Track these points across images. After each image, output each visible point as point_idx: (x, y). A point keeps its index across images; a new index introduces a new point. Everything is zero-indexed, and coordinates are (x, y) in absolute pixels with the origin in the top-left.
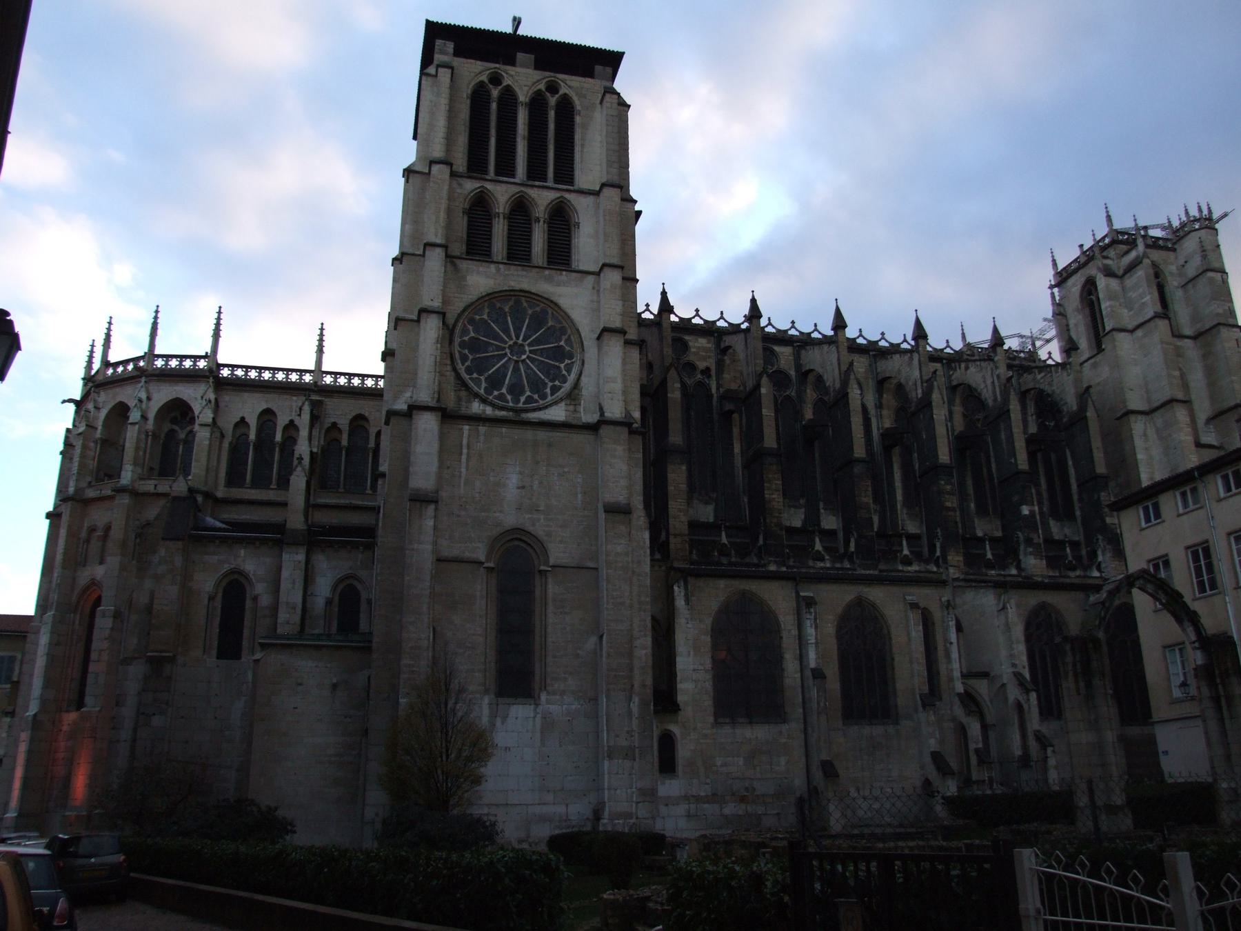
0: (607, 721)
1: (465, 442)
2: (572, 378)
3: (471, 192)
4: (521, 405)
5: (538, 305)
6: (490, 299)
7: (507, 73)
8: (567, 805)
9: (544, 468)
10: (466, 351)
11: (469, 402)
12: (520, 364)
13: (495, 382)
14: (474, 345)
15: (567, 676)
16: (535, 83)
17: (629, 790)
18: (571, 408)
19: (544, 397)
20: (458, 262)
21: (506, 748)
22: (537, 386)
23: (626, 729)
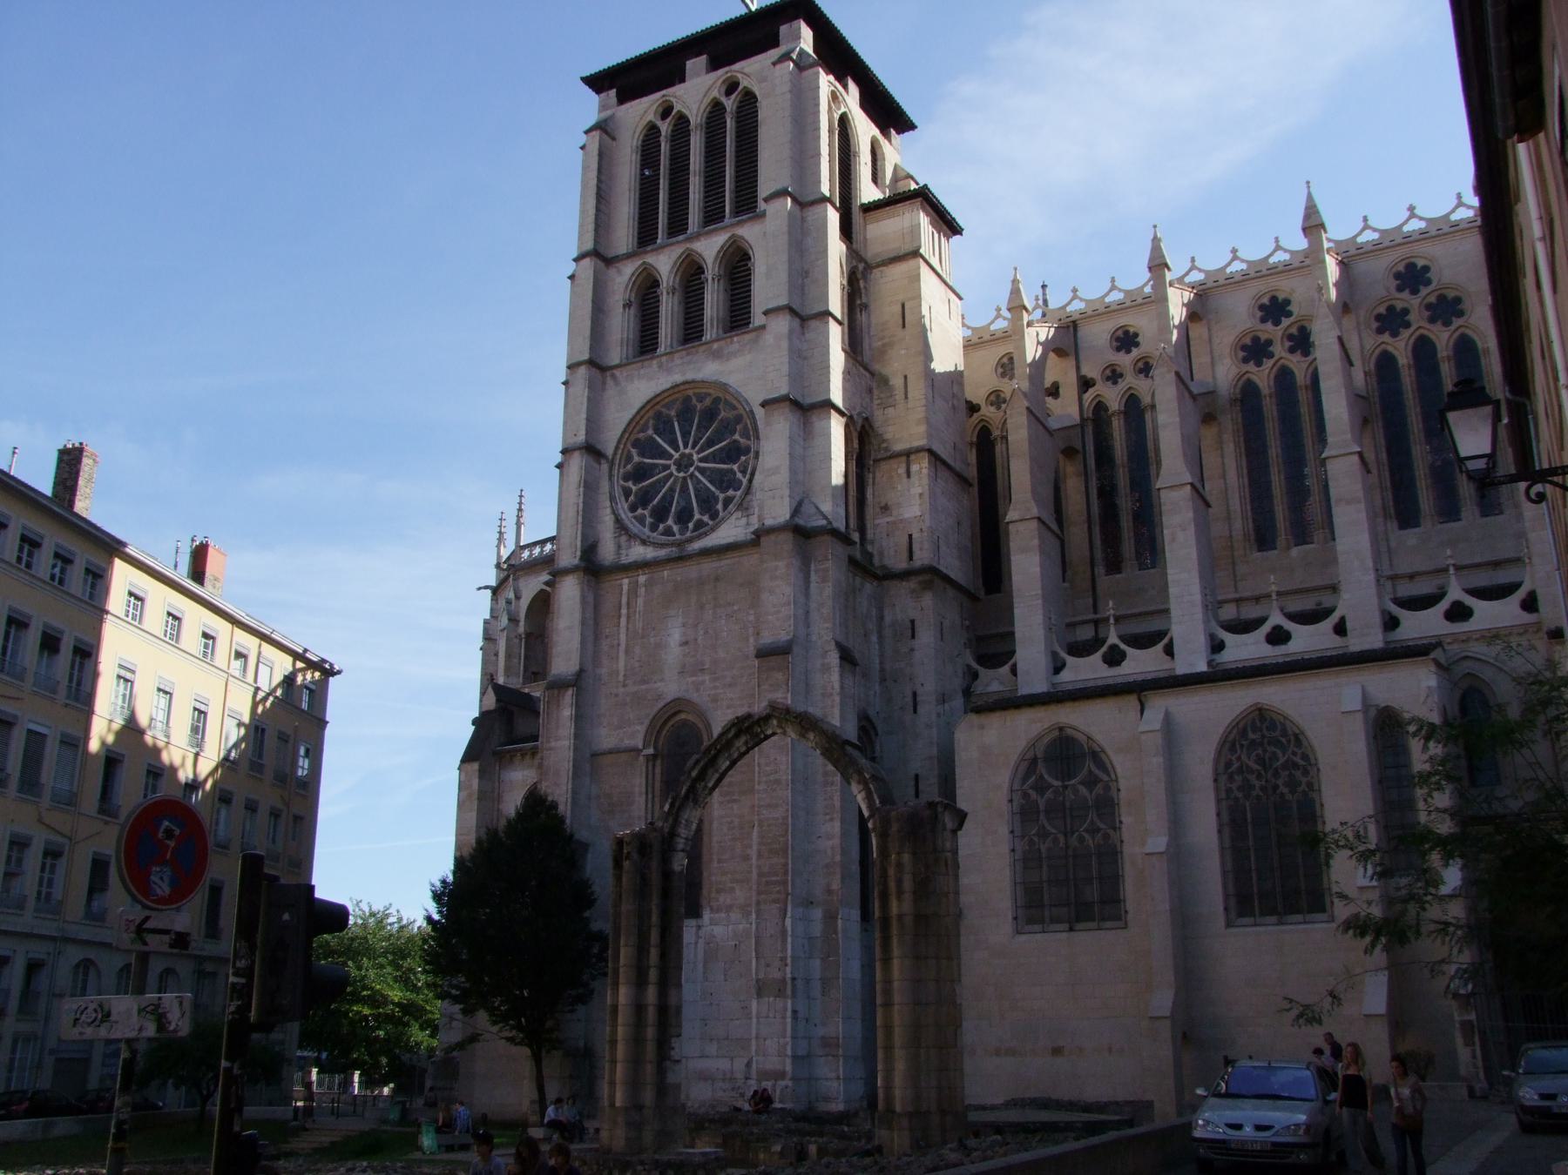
1: (624, 600)
2: (745, 481)
3: (633, 274)
4: (688, 534)
6: (652, 407)
7: (675, 97)
8: (732, 1059)
10: (630, 484)
11: (629, 547)
12: (689, 481)
13: (660, 514)
14: (640, 474)
16: (707, 92)
17: (782, 1040)
18: (744, 520)
19: (714, 516)
20: (617, 372)
22: (707, 503)
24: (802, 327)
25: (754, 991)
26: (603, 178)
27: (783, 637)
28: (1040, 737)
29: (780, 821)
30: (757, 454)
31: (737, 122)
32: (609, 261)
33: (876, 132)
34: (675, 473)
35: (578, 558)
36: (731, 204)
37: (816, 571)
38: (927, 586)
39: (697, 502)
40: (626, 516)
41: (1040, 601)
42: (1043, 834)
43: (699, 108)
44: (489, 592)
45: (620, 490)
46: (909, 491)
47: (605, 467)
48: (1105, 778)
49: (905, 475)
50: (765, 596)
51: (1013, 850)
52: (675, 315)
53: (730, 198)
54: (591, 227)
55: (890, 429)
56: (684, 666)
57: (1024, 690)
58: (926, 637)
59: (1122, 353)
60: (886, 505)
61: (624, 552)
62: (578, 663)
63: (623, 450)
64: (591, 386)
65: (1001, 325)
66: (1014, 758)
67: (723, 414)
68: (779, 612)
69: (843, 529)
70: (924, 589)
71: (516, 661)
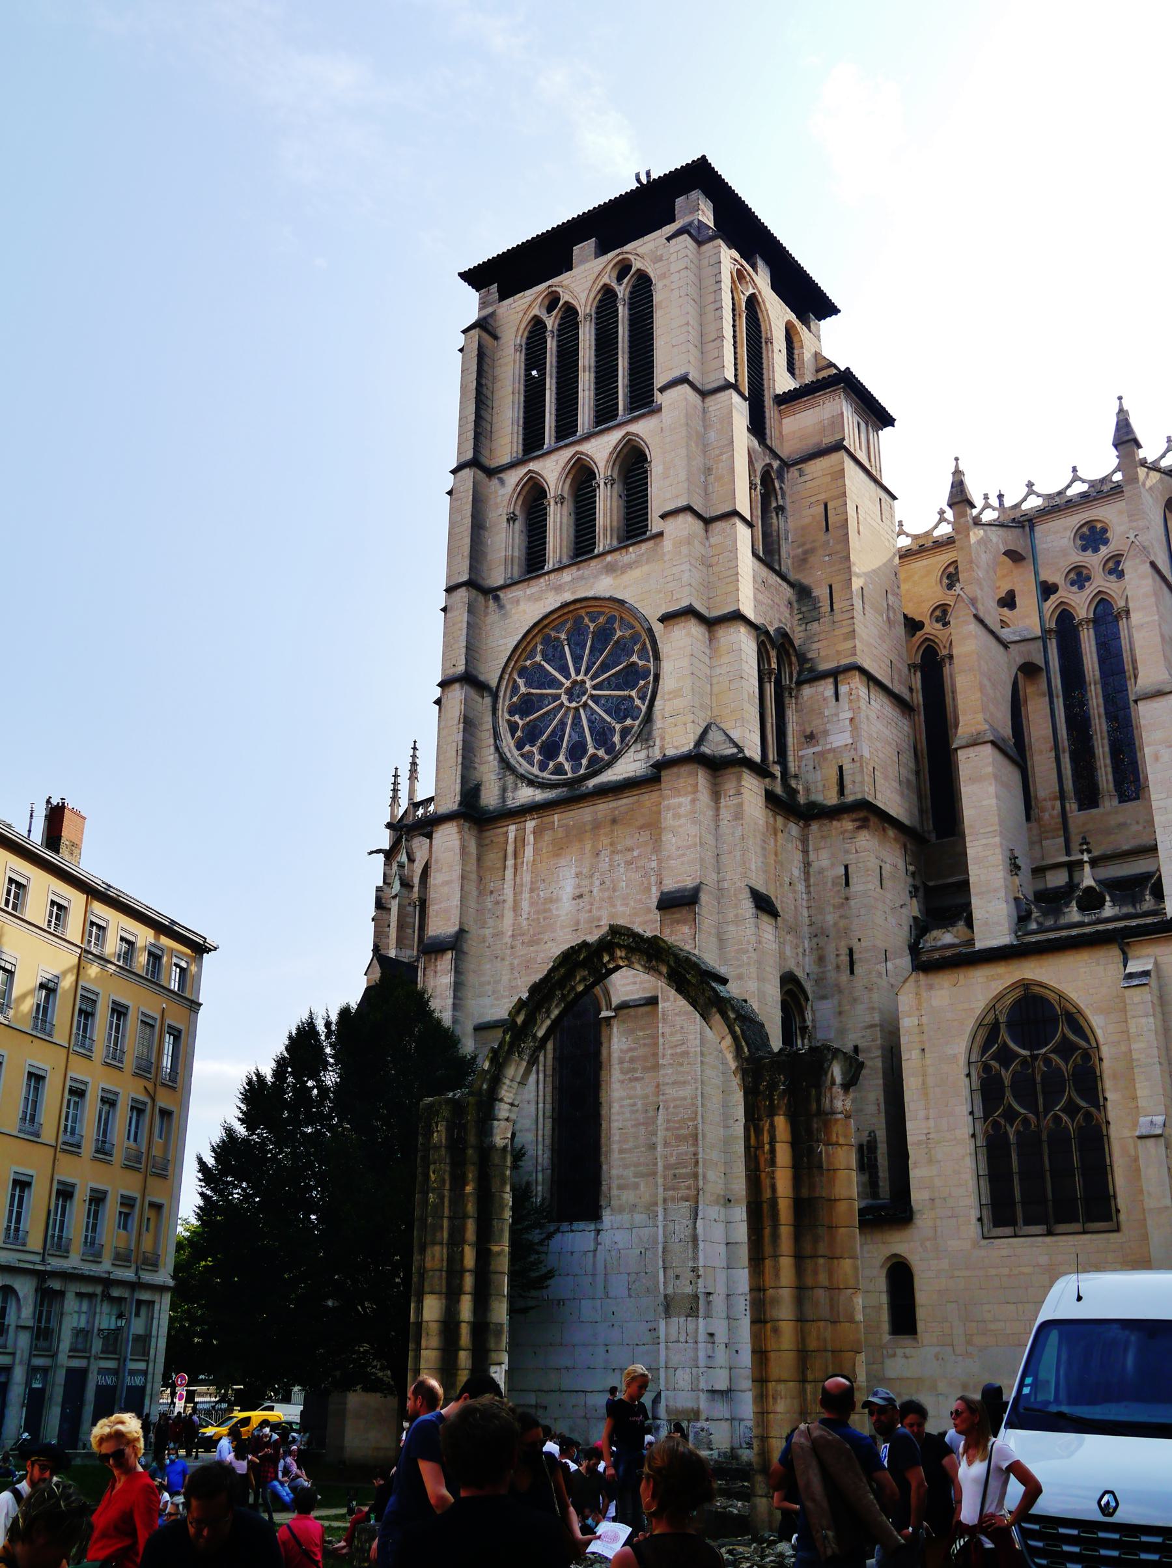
0: (663, 1252)
1: (510, 849)
2: (644, 708)
3: (517, 485)
4: (582, 771)
5: (602, 613)
6: (540, 631)
9: (607, 859)
10: (517, 718)
11: (516, 788)
12: (582, 711)
13: (550, 751)
14: (526, 706)
15: (636, 1180)
17: (695, 1370)
18: (643, 754)
19: (610, 749)
20: (501, 594)
21: (559, 1301)
22: (602, 736)
23: (691, 1264)
24: (707, 531)
25: (661, 1308)
26: (484, 382)
27: (689, 883)
28: (999, 998)
29: (689, 1101)
30: (657, 678)
31: (630, 309)
32: (492, 472)
33: (792, 317)
34: (566, 703)
35: (457, 803)
36: (624, 400)
37: (726, 806)
38: (863, 825)
39: (592, 736)
40: (513, 755)
41: (997, 839)
42: (1010, 1115)
43: (587, 298)
44: (381, 855)
45: (506, 725)
46: (837, 715)
47: (488, 700)
48: (1083, 1043)
49: (834, 700)
50: (667, 837)
51: (973, 1136)
52: (565, 528)
53: (624, 395)
54: (471, 434)
55: (815, 646)
56: (577, 923)
57: (982, 942)
58: (863, 884)
59: (1089, 552)
60: (812, 732)
61: (509, 795)
62: (457, 923)
63: (508, 680)
64: (471, 610)
65: (945, 529)
66: (970, 1024)
67: (619, 633)
68: (683, 855)
69: (757, 758)
70: (859, 828)
71: (410, 931)
